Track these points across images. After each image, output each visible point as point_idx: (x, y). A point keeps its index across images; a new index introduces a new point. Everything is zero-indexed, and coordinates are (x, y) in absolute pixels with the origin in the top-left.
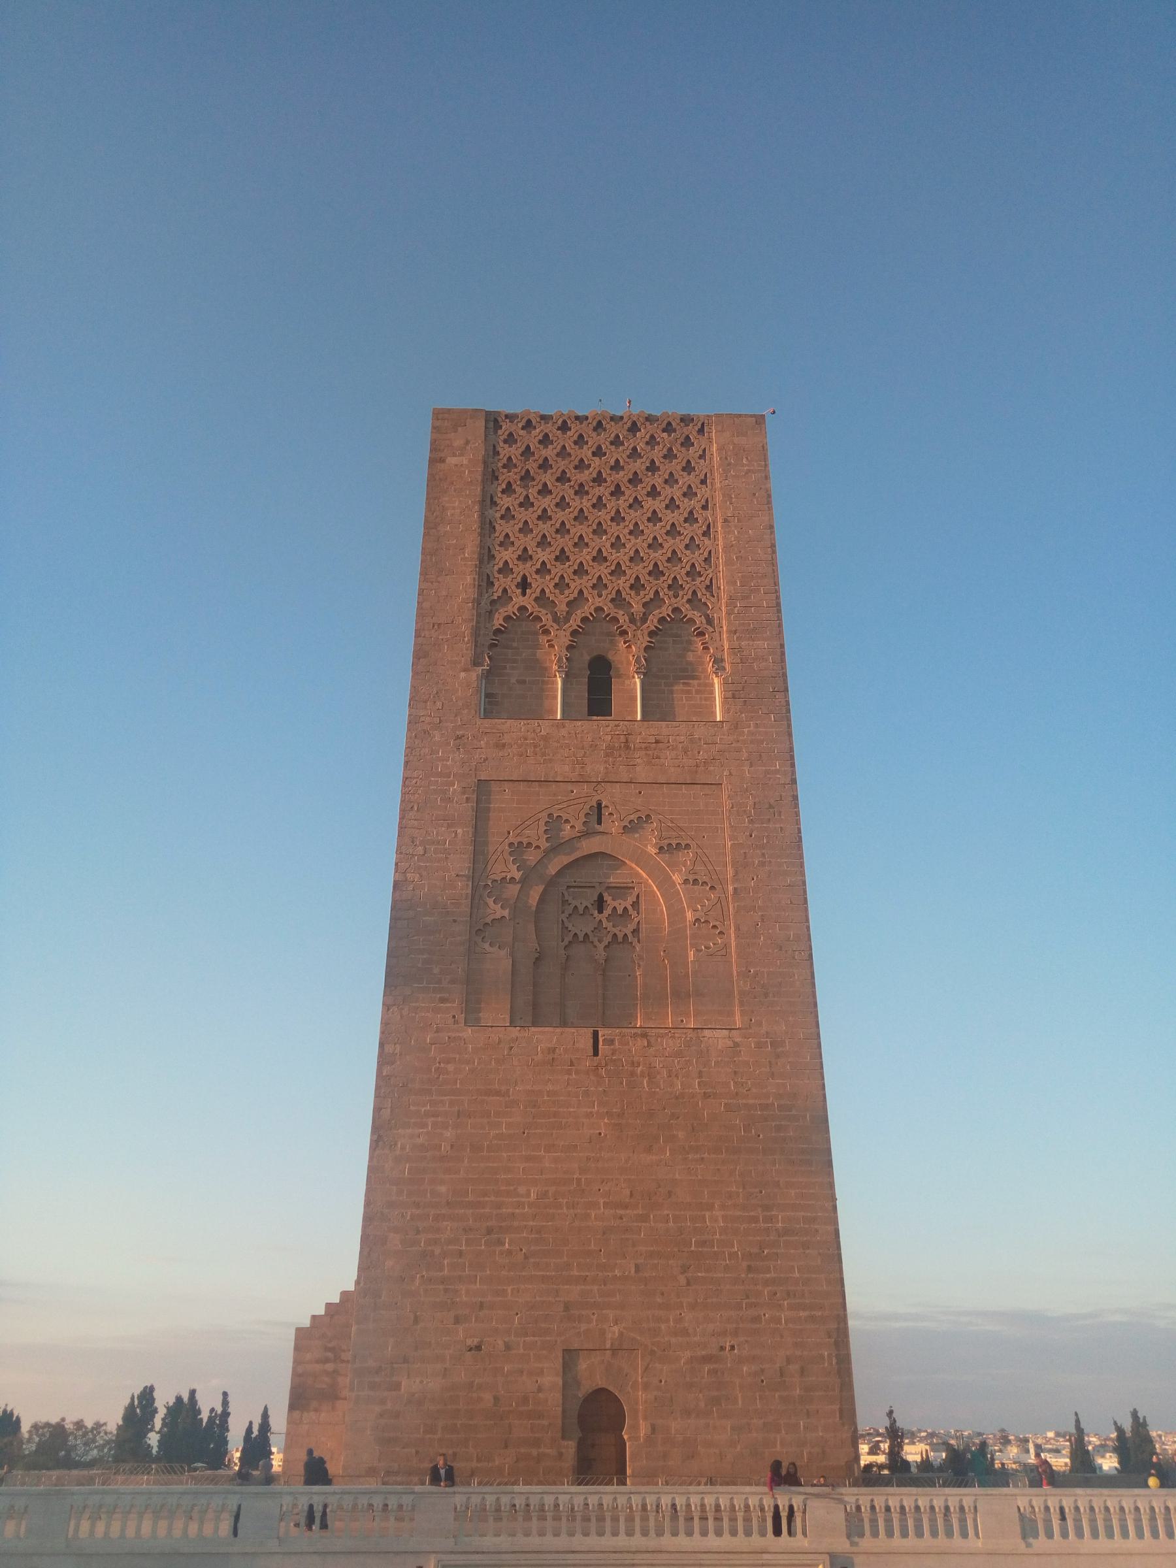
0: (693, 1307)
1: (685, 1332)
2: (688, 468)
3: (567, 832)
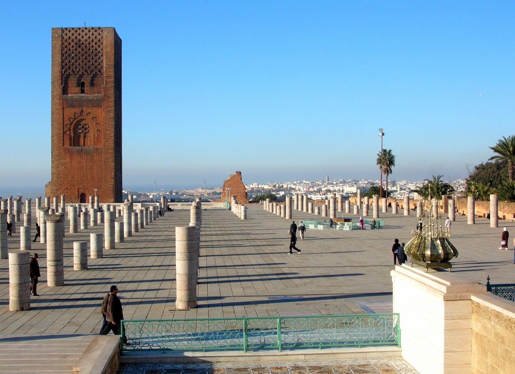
3: (77, 115)
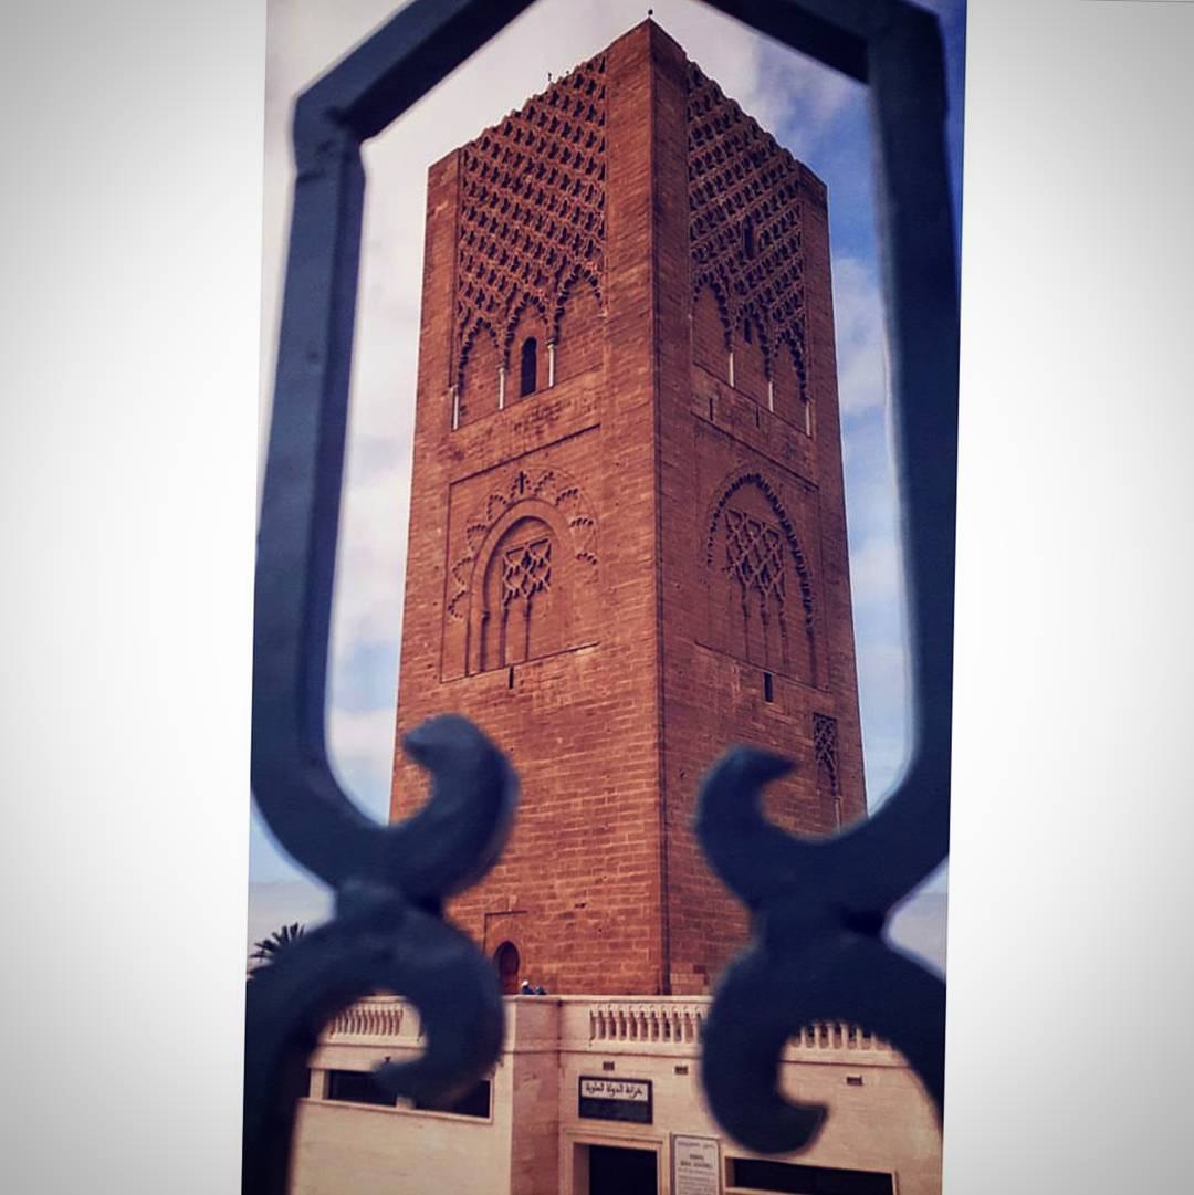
0: (560, 876)
1: (553, 896)
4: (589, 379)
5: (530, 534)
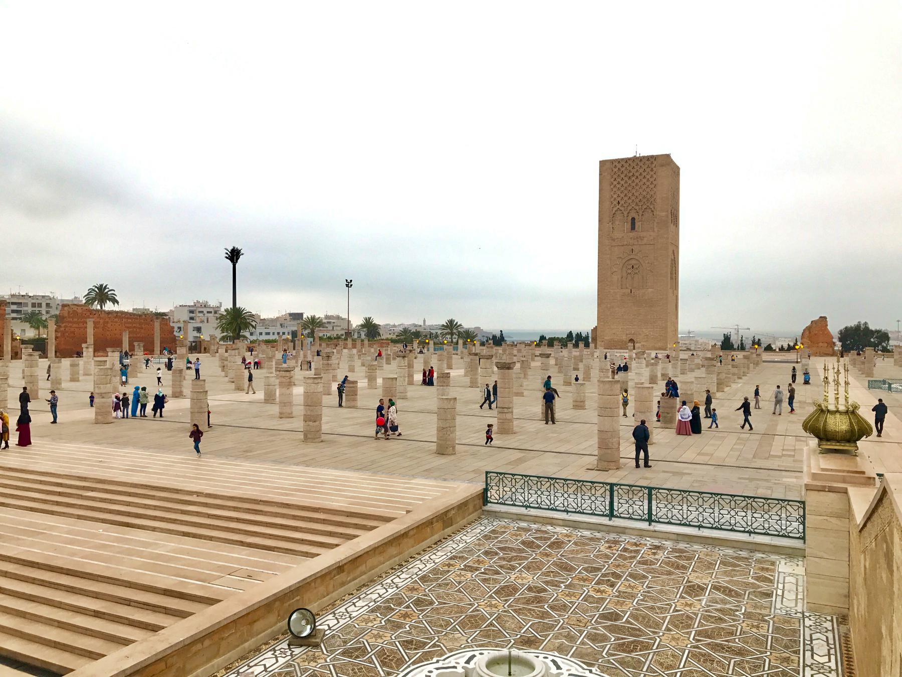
2: (652, 170)
4: (652, 233)
5: (633, 262)
